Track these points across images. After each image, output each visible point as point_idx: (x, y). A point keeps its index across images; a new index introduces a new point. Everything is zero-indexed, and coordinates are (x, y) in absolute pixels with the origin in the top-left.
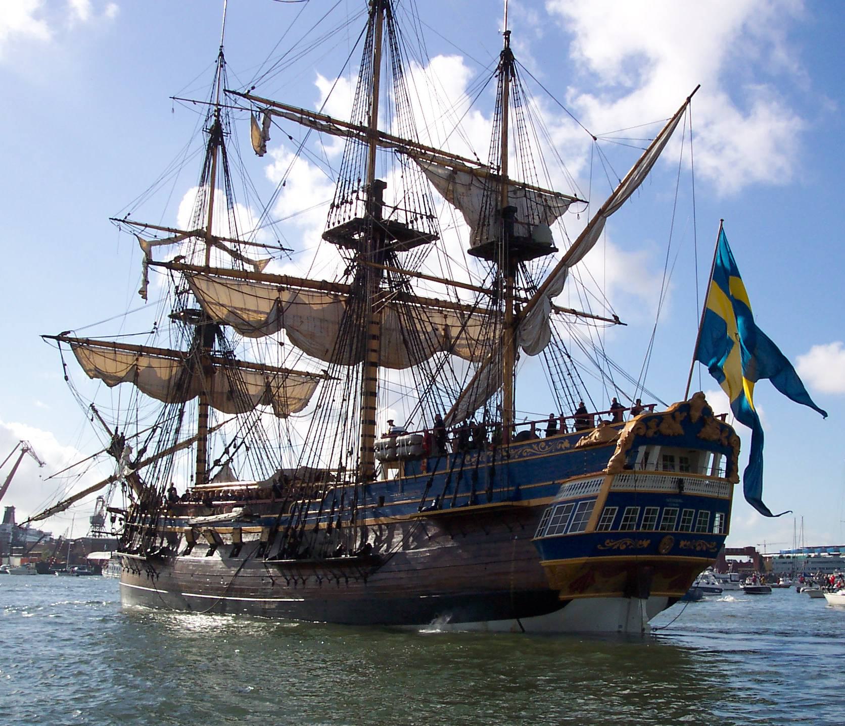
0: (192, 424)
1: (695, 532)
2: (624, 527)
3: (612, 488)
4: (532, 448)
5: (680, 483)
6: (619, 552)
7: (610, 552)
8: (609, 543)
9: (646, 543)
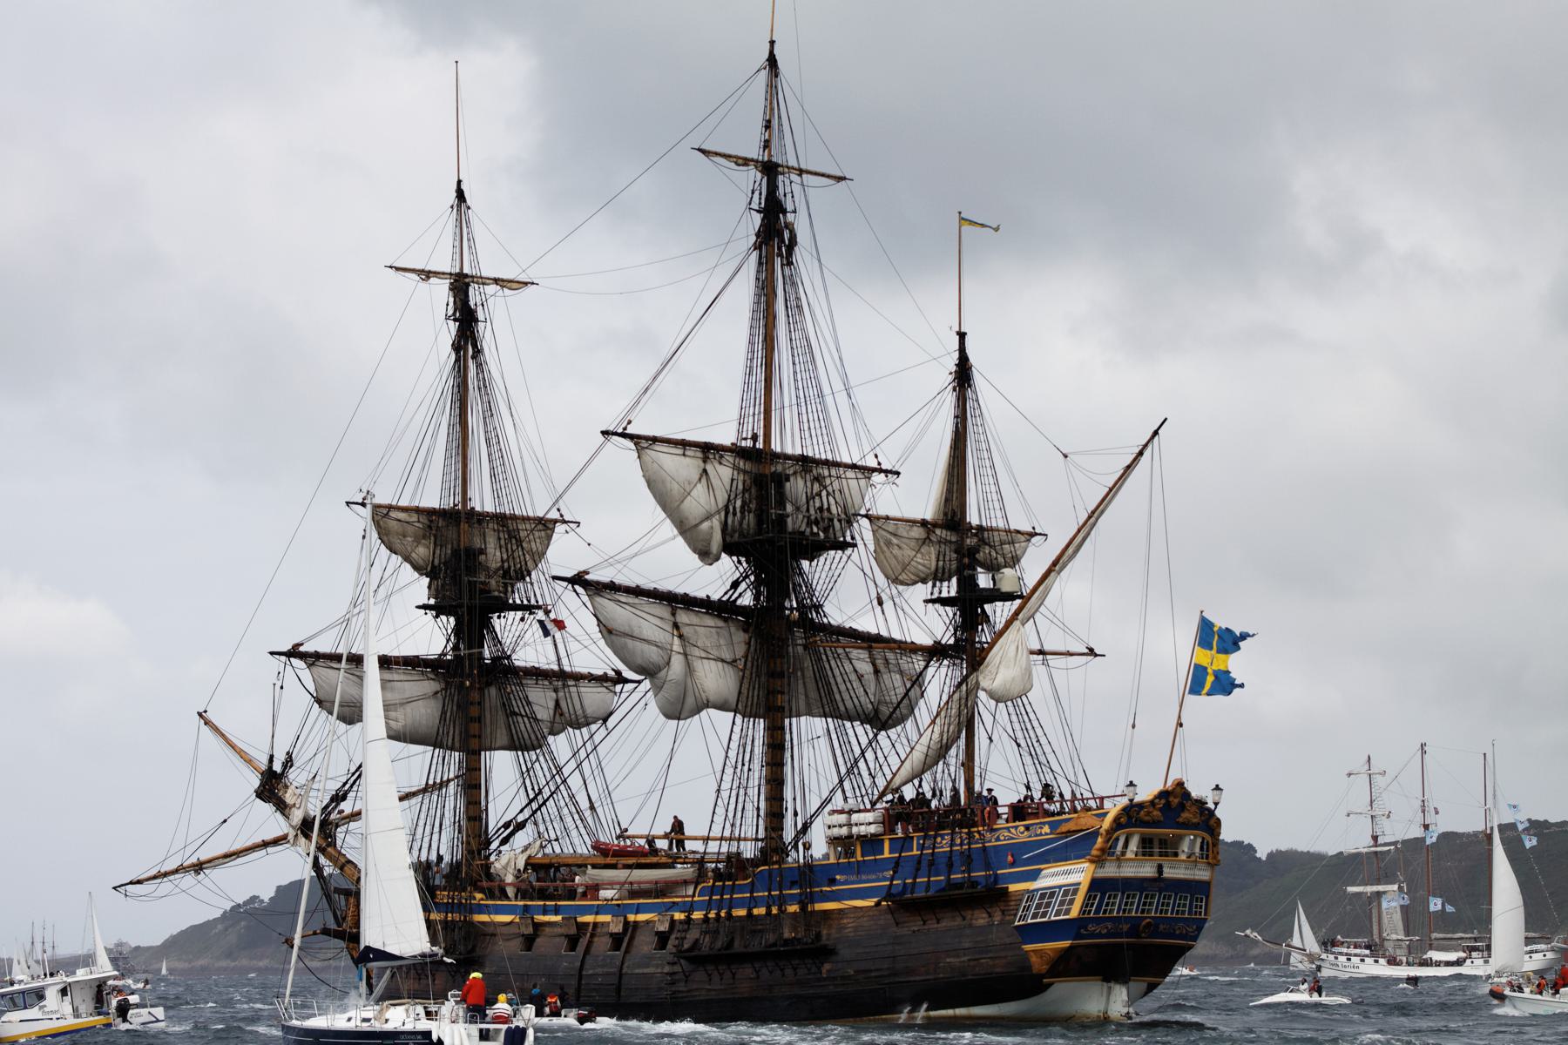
7: (1092, 936)
8: (1091, 928)
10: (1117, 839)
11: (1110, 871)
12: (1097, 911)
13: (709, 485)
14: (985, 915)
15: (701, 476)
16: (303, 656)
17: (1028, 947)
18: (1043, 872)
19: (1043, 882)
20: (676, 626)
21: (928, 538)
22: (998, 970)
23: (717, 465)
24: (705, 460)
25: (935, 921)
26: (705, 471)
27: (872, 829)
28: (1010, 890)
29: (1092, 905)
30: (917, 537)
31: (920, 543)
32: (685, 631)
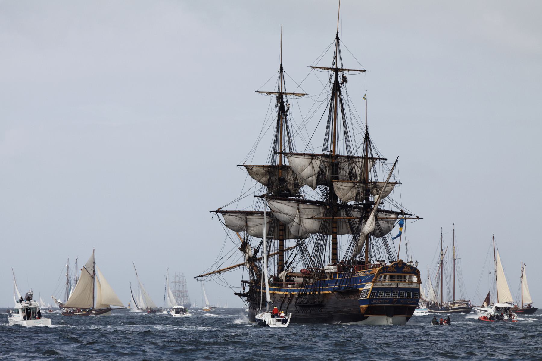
0: (260, 263)
1: (400, 298)
2: (379, 297)
3: (374, 286)
4: (361, 273)
5: (397, 284)
6: (378, 303)
8: (374, 301)
9: (388, 301)
10: (381, 277)
11: (379, 285)
12: (376, 296)
13: (313, 166)
14: (354, 297)
15: (310, 164)
16: (221, 212)
17: (361, 306)
18: (366, 285)
19: (365, 288)
20: (298, 209)
21: (354, 186)
22: (355, 312)
23: (316, 160)
24: (312, 159)
25: (344, 298)
26: (311, 162)
27: (333, 271)
28: (360, 290)
29: (374, 295)
30: (350, 186)
31: (351, 188)
32: (301, 210)
